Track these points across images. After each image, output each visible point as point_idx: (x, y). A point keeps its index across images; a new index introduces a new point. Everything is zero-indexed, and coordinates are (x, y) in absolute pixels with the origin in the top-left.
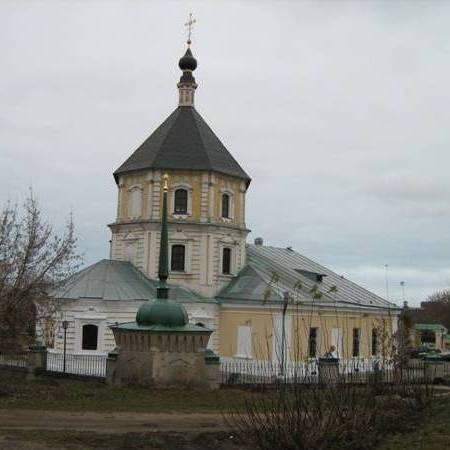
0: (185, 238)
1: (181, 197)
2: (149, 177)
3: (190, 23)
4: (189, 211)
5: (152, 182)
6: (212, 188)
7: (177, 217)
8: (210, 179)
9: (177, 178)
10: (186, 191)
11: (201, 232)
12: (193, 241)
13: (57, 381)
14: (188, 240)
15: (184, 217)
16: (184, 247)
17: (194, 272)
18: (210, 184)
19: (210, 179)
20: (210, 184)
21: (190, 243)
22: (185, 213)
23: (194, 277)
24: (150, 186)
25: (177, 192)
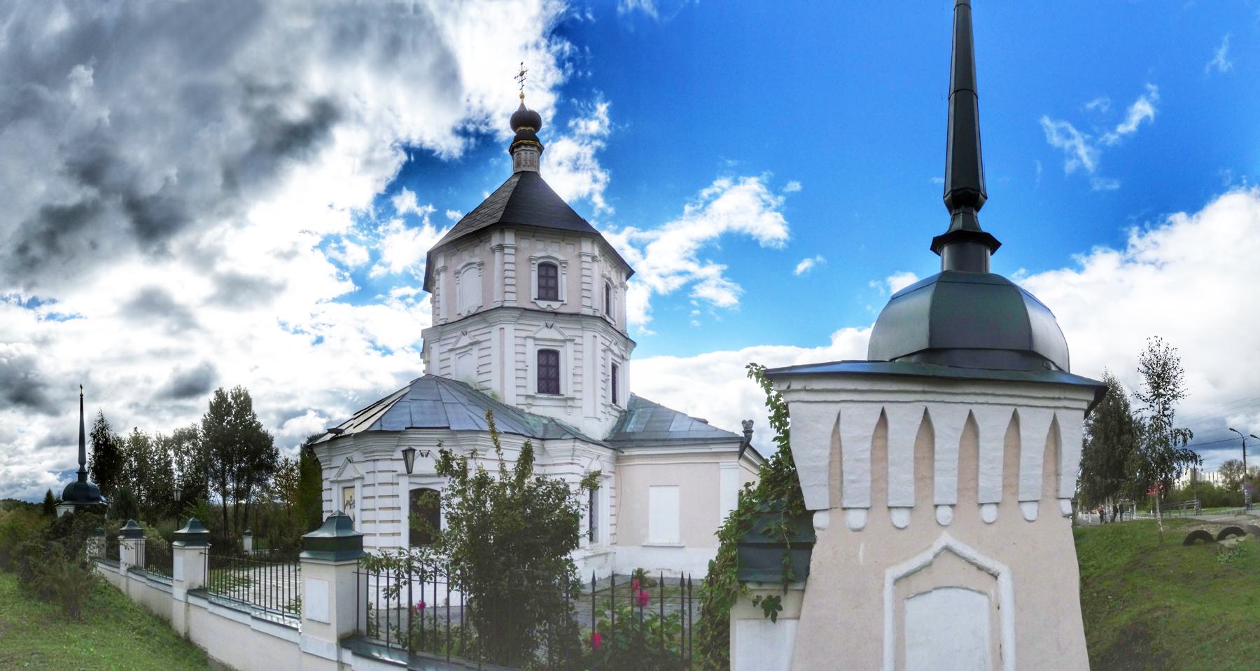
0: (562, 338)
1: (548, 274)
2: (496, 240)
3: (522, 74)
4: (563, 293)
5: (501, 247)
6: (596, 264)
7: (543, 304)
8: (593, 249)
9: (540, 245)
10: (555, 267)
11: (583, 329)
12: (573, 340)
13: (437, 624)
14: (564, 341)
15: (555, 305)
16: (556, 354)
17: (578, 395)
18: (594, 258)
19: (593, 249)
20: (594, 258)
21: (569, 345)
22: (556, 299)
23: (577, 403)
24: (497, 254)
25: (540, 266)
